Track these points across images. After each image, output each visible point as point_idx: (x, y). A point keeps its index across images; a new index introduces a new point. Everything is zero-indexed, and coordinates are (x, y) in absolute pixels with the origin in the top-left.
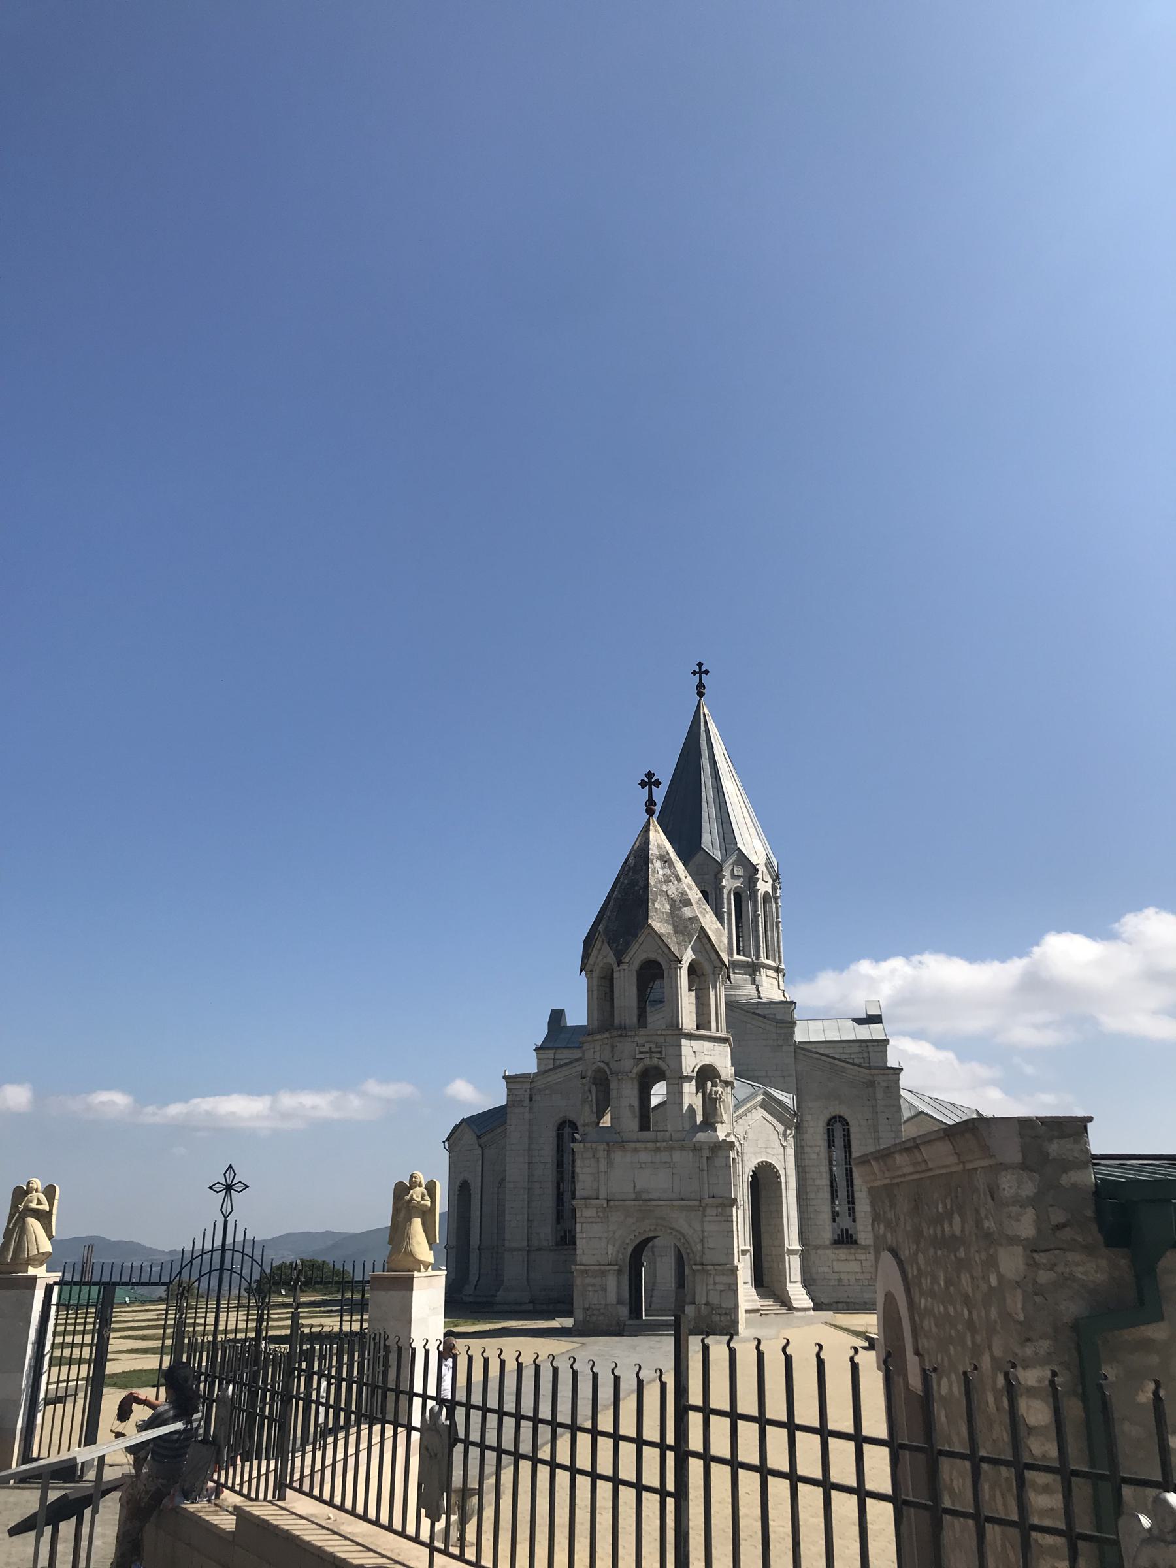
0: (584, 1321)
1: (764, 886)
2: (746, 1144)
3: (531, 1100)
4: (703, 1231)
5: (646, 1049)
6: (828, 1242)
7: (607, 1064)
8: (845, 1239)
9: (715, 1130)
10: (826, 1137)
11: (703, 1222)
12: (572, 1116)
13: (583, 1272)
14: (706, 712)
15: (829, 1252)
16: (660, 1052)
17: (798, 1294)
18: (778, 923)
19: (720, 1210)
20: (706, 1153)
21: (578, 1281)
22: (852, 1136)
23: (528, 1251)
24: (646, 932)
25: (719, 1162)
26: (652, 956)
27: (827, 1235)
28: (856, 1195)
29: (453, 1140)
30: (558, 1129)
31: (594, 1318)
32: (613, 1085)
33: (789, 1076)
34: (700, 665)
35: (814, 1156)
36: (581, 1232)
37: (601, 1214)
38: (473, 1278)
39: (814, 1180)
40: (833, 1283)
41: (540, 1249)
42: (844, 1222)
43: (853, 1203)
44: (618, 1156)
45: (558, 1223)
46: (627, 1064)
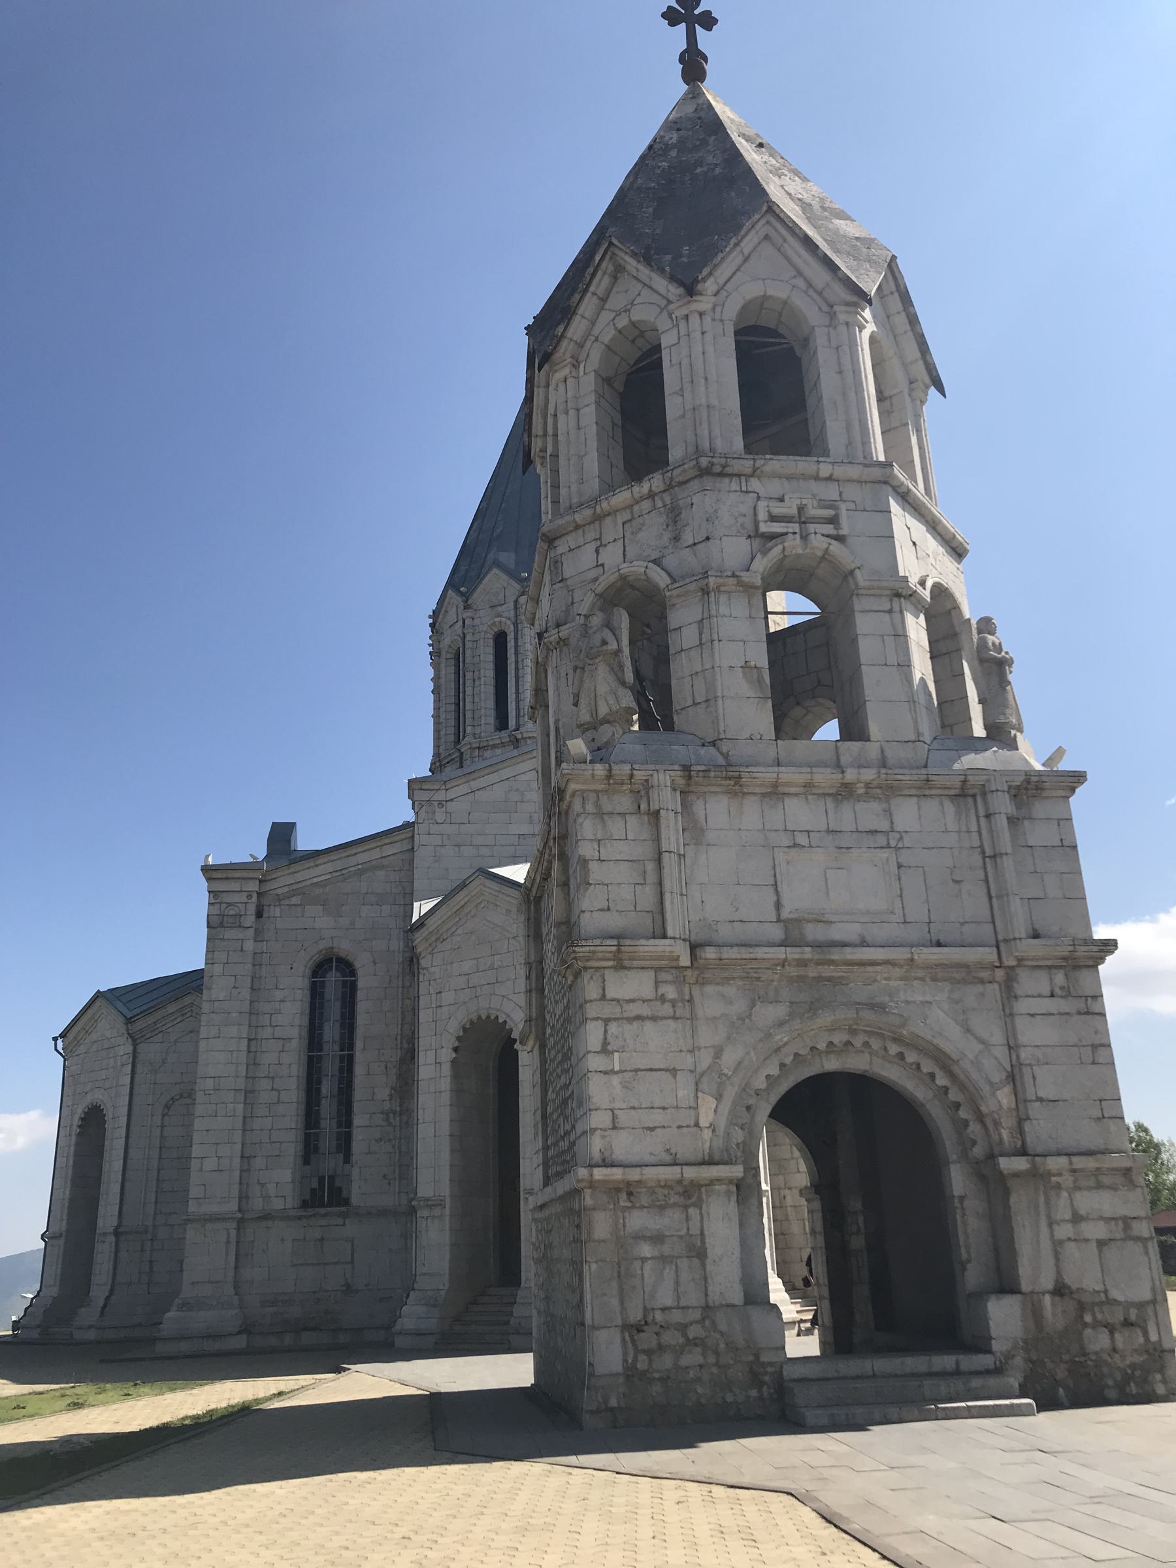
0: (631, 1374)
3: (259, 914)
4: (1012, 1047)
5: (789, 508)
7: (654, 562)
9: (1012, 745)
11: (1009, 1016)
12: (344, 947)
13: (614, 1190)
16: (834, 521)
19: (1060, 978)
20: (1003, 805)
21: (601, 1225)
23: (241, 1221)
24: (761, 229)
25: (1039, 834)
26: (778, 291)
29: (71, 1039)
30: (314, 974)
31: (666, 1362)
32: (683, 617)
36: (605, 1050)
37: (670, 992)
38: (98, 1293)
41: (266, 1217)
44: (716, 810)
45: (306, 1160)
46: (732, 550)
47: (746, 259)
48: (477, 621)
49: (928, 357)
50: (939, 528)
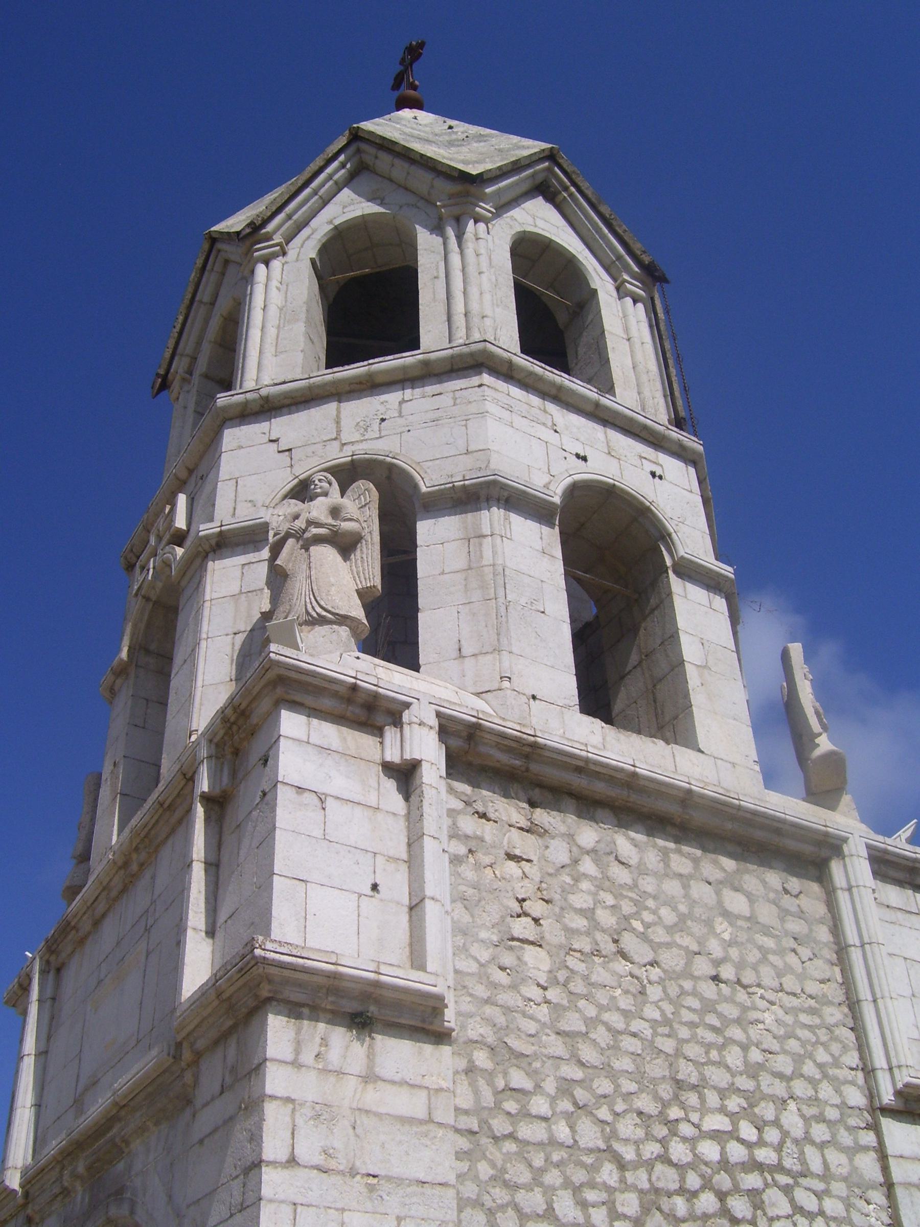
47: (213, 304)
50: (379, 380)
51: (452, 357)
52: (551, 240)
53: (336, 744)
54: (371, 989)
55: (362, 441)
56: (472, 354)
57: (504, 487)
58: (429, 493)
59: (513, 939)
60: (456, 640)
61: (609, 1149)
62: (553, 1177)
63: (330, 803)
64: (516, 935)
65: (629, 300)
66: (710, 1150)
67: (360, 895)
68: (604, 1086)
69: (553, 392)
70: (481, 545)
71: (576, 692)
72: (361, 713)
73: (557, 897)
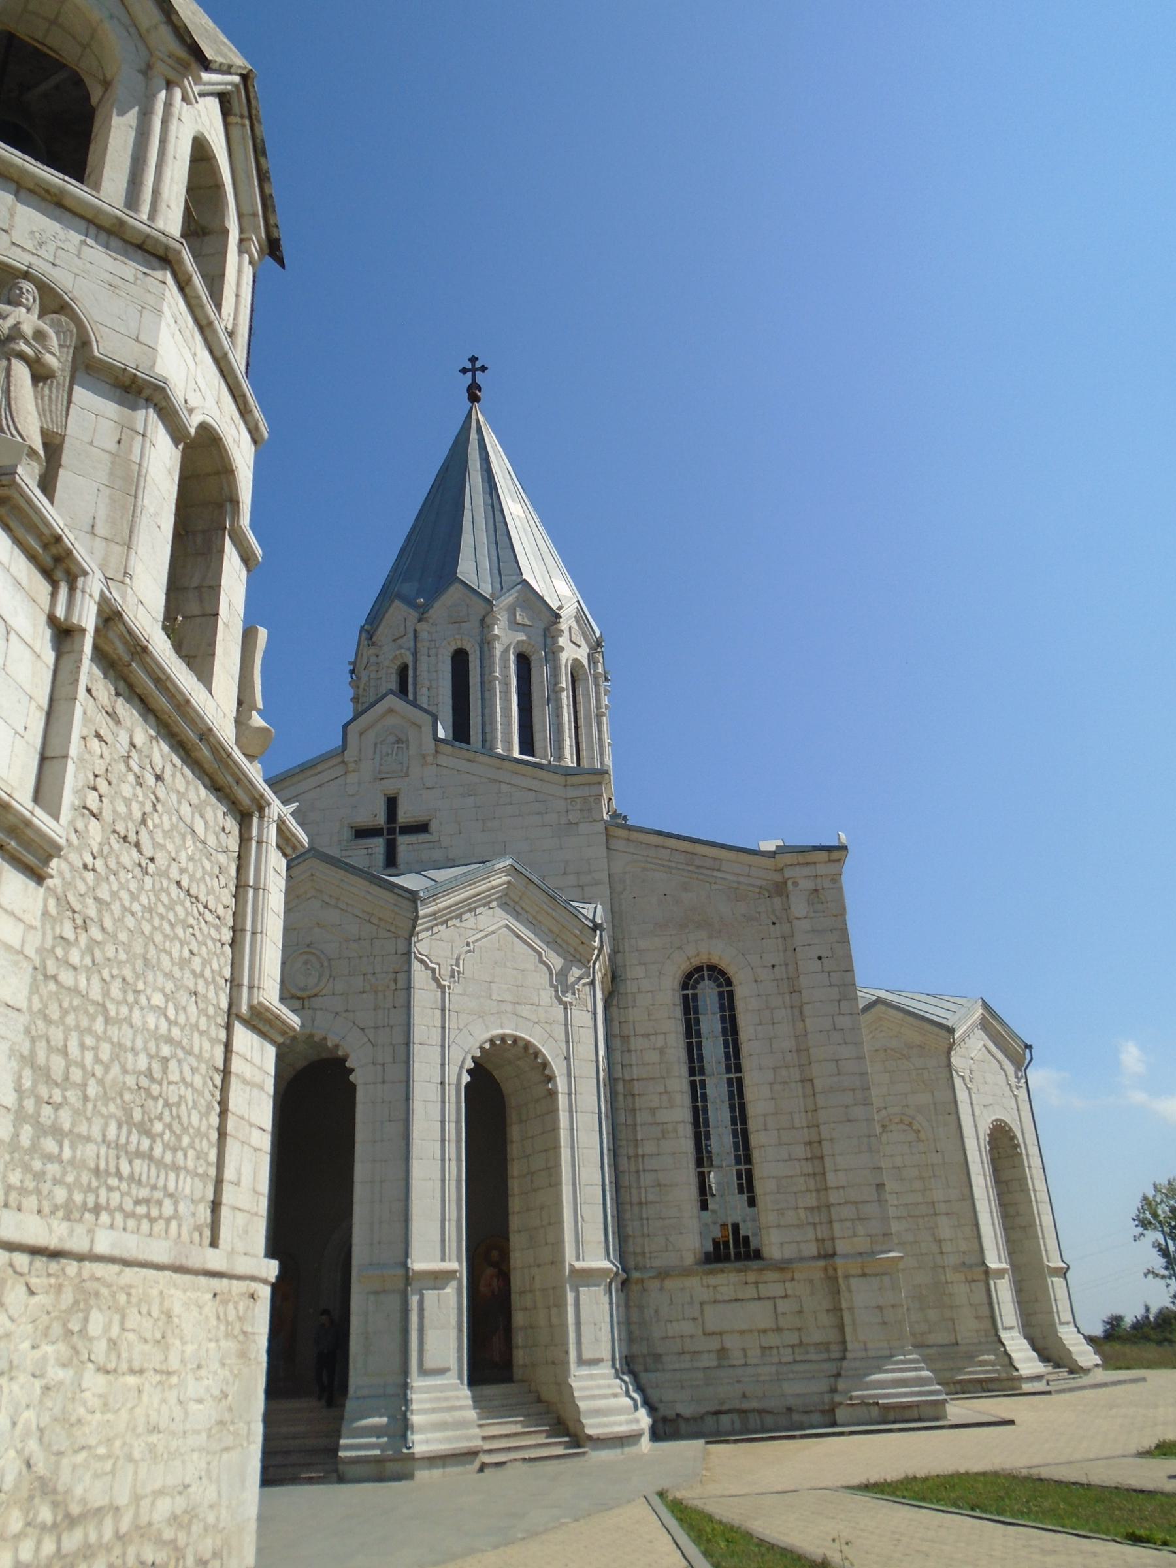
1: (572, 651)
2: (458, 989)
6: (689, 1259)
8: (733, 1250)
10: (679, 1012)
14: (481, 419)
15: (693, 1282)
17: (603, 1398)
18: (599, 716)
22: (740, 1006)
27: (690, 1237)
28: (754, 1139)
33: (596, 883)
34: (473, 359)
35: (654, 1057)
39: (653, 1111)
40: (709, 1361)
42: (730, 1207)
43: (748, 1159)
48: (381, 658)
49: (174, 18)
51: (148, 236)
52: (214, 157)
53: (24, 583)
54: (22, 826)
55: (33, 254)
56: (167, 248)
57: (167, 397)
58: (101, 360)
59: (85, 807)
60: (91, 515)
61: (104, 1006)
62: (70, 1020)
63: (13, 636)
64: (88, 805)
65: (246, 257)
66: (151, 1021)
67: (16, 733)
68: (110, 951)
69: (204, 323)
70: (133, 439)
71: (162, 610)
72: (48, 561)
73: (114, 782)
